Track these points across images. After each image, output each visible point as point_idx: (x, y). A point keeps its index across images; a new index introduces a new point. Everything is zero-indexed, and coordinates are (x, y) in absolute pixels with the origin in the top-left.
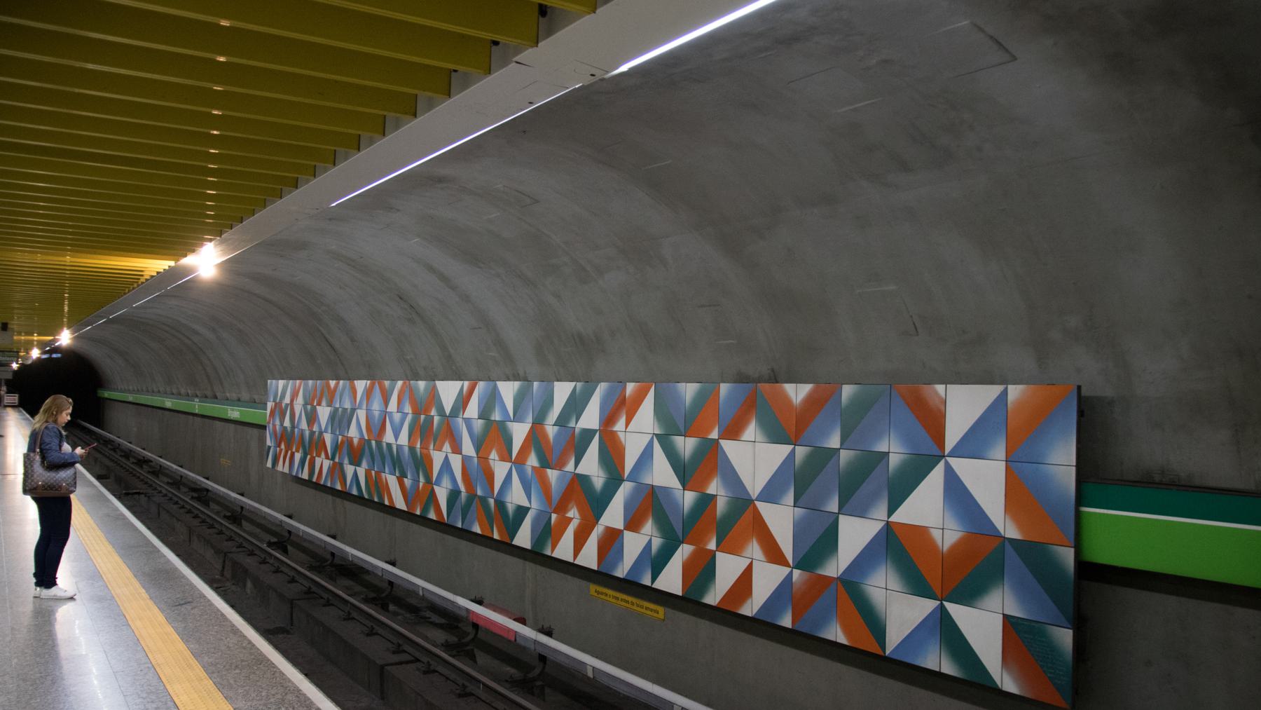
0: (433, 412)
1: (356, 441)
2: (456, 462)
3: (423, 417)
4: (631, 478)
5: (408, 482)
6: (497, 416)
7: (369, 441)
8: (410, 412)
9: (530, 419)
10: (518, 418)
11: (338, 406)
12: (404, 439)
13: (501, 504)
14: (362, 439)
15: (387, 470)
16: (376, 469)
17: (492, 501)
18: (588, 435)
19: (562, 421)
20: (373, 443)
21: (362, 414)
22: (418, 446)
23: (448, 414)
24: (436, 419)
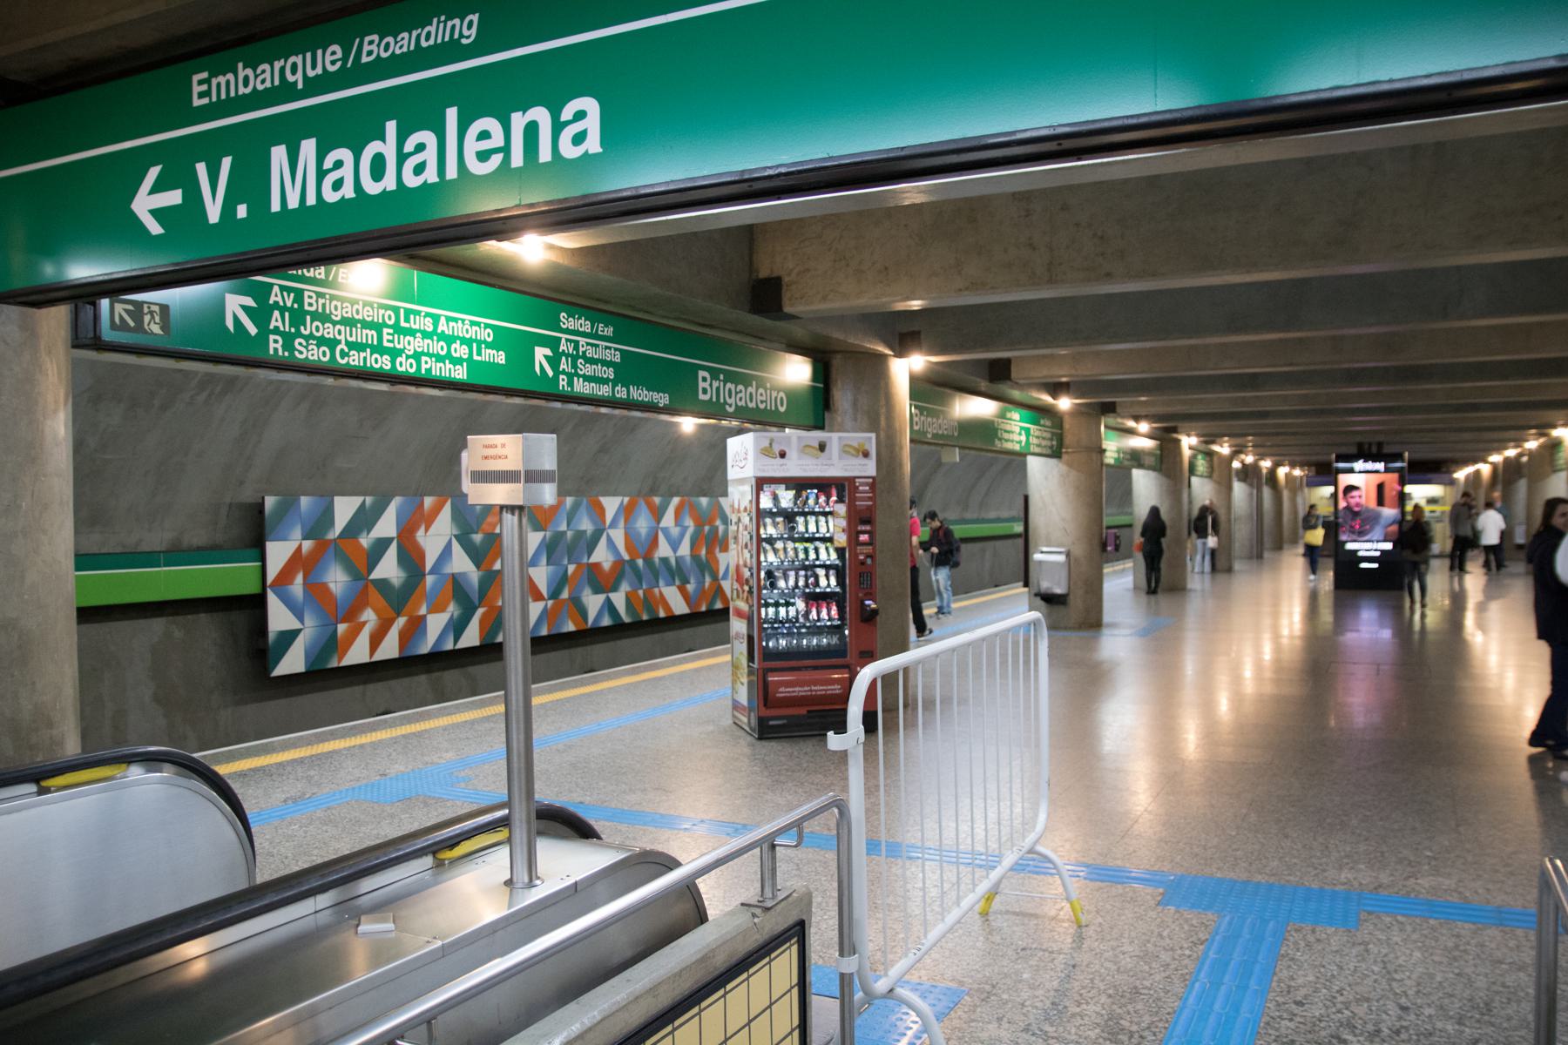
7: (632, 562)
16: (644, 587)
21: (618, 536)
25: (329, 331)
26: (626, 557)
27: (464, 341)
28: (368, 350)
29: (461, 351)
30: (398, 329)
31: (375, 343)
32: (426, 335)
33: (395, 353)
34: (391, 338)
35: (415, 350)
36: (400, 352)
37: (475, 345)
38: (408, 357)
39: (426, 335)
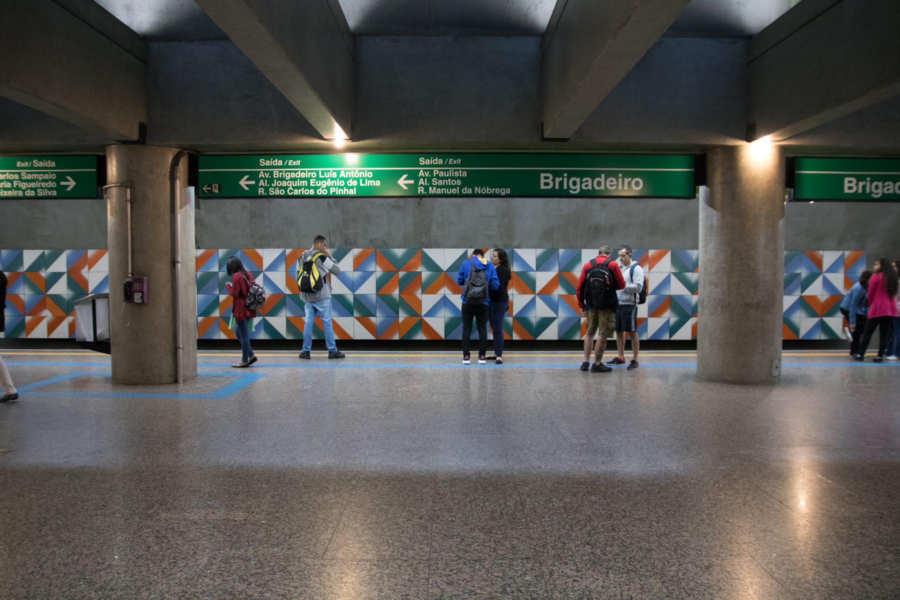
12: (369, 288)
22: (396, 293)
25: (284, 184)
26: (288, 292)
27: (354, 179)
28: (303, 188)
29: (355, 183)
30: (318, 179)
31: (306, 185)
32: (332, 179)
33: (316, 188)
34: (314, 182)
35: (327, 186)
36: (319, 187)
37: (361, 180)
38: (323, 189)
39: (332, 179)
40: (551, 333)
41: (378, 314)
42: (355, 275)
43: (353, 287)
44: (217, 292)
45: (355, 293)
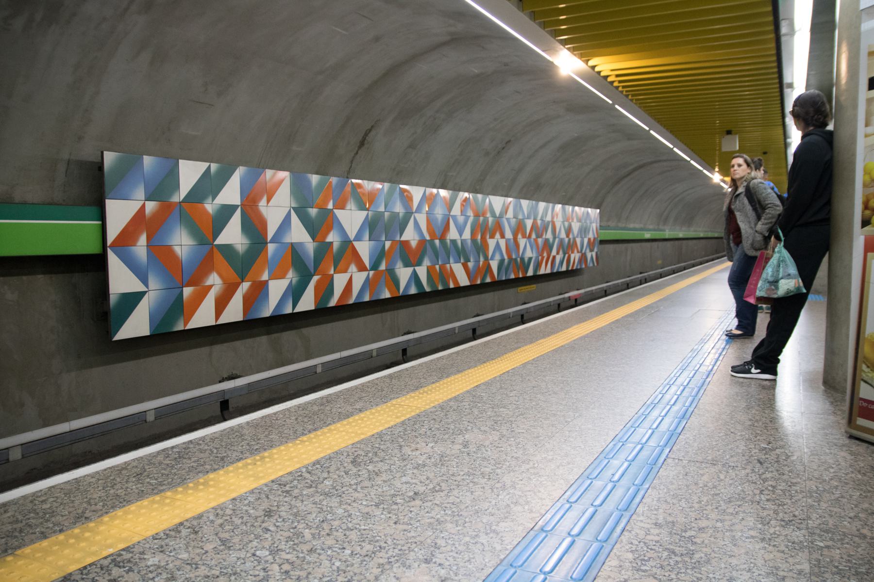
0: (488, 215)
1: (414, 244)
2: (502, 243)
3: (481, 218)
4: (558, 237)
5: (471, 265)
6: (520, 217)
8: (472, 215)
9: (532, 218)
10: (528, 218)
11: (382, 209)
12: (467, 235)
13: (522, 259)
14: (422, 242)
15: (451, 260)
16: (440, 263)
17: (519, 259)
18: (549, 222)
19: (542, 219)
20: (437, 242)
21: (422, 219)
23: (498, 215)
24: (491, 220)
26: (428, 238)
40: (530, 273)
41: (472, 260)
42: (461, 219)
43: (461, 232)
44: (384, 239)
45: (462, 238)
